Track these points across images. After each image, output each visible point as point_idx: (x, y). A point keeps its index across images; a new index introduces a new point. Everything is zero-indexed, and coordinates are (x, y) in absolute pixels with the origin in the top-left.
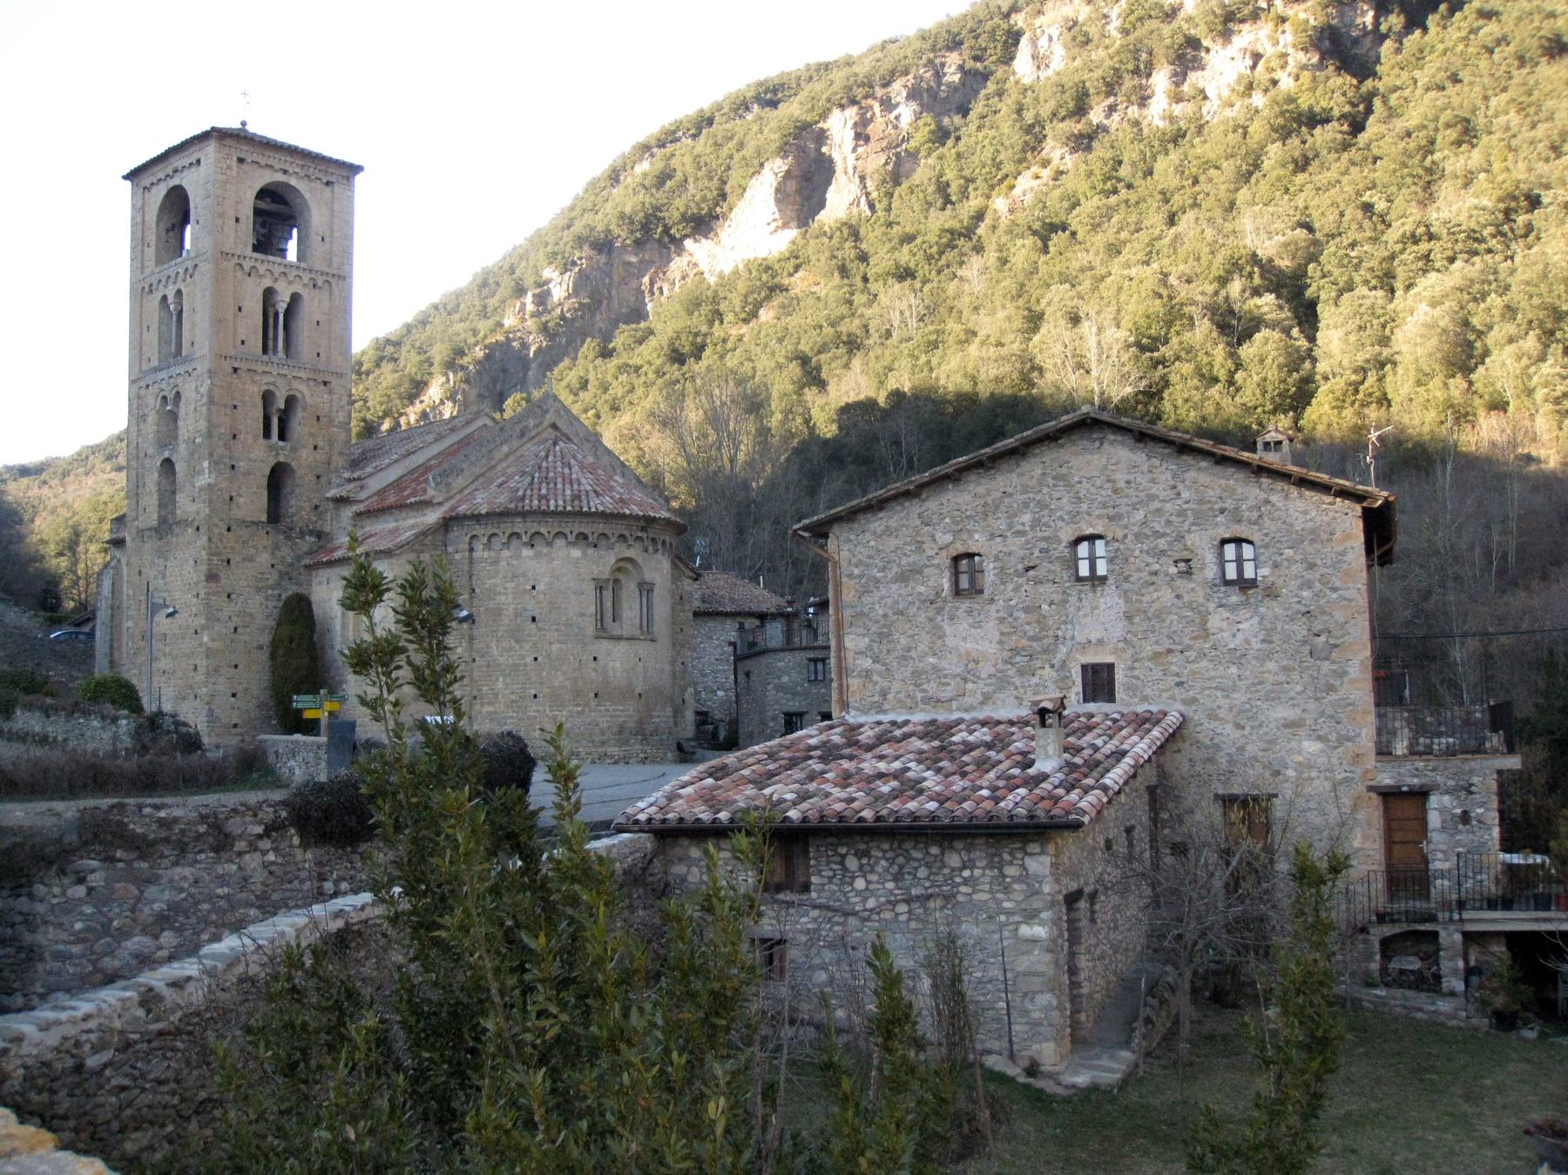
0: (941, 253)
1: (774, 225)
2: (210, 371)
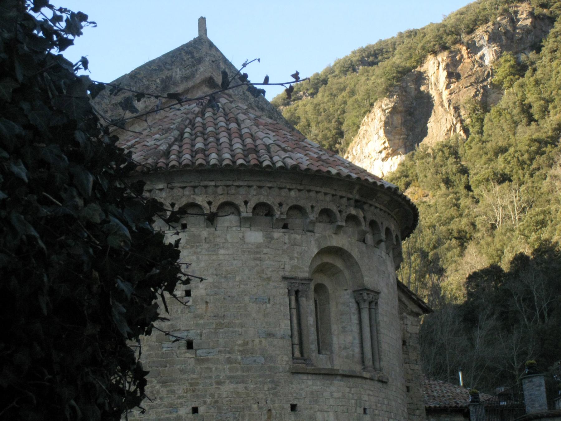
0: (532, 159)
1: (384, 154)
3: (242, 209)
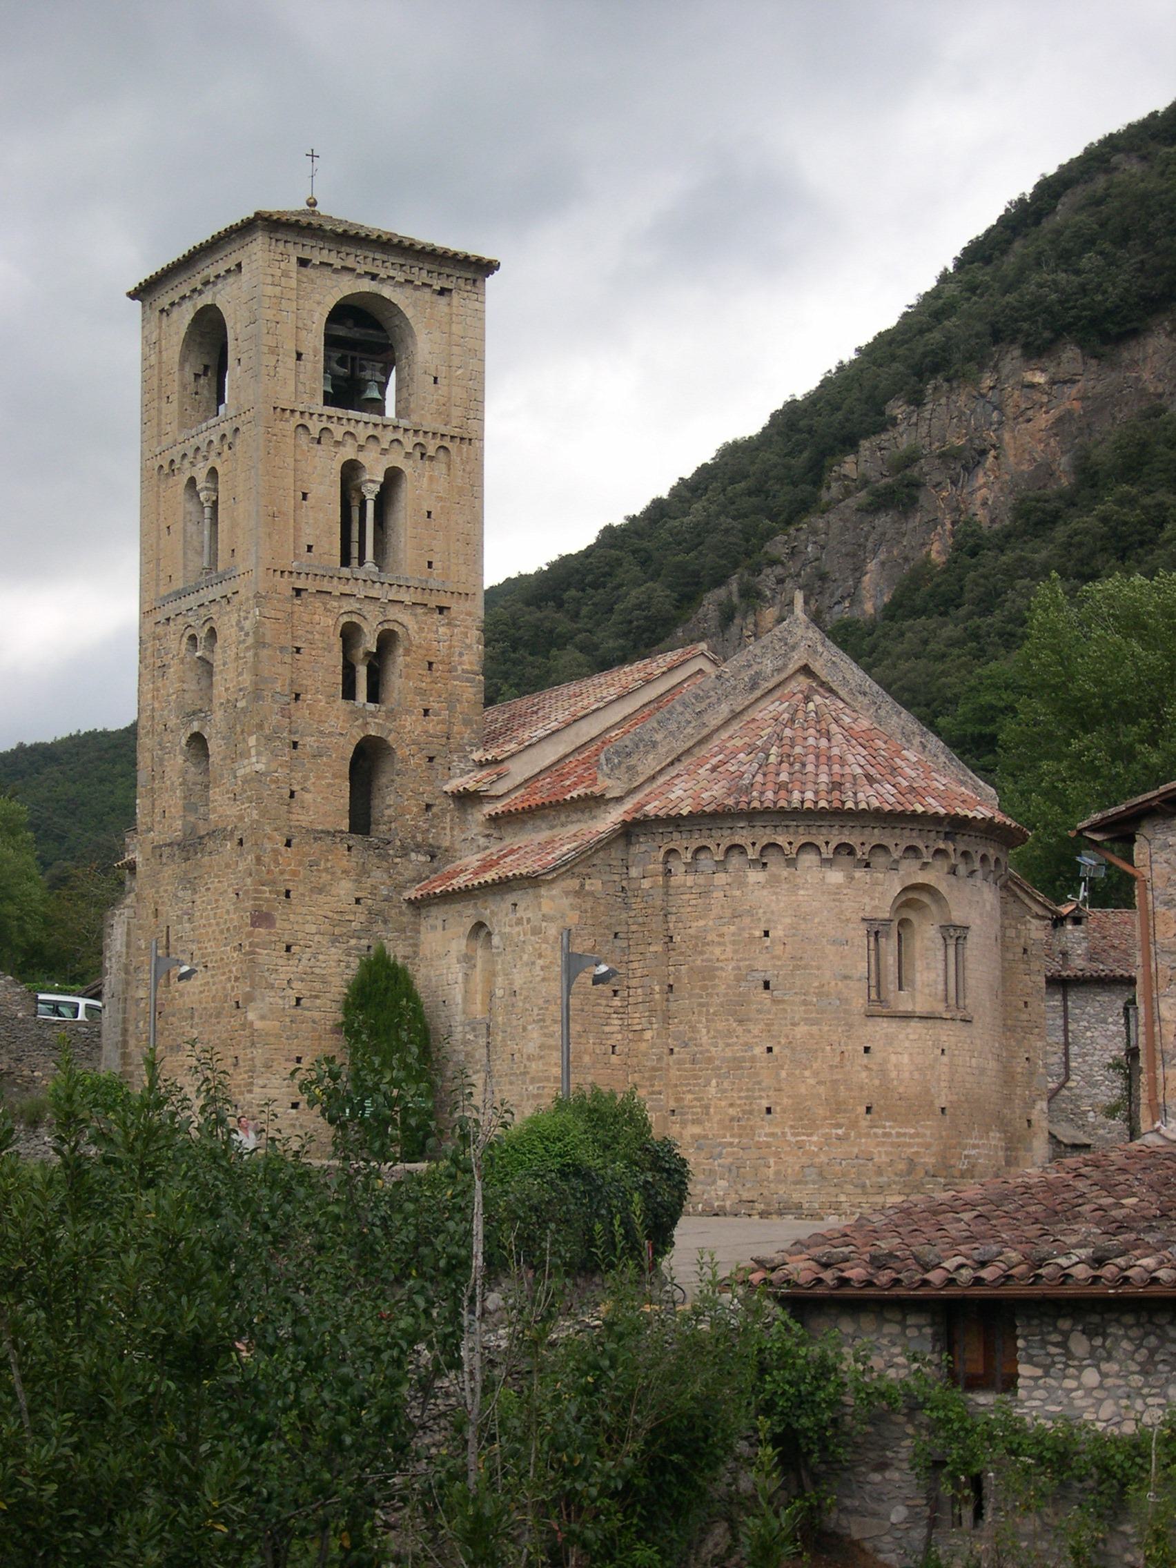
2: (257, 596)
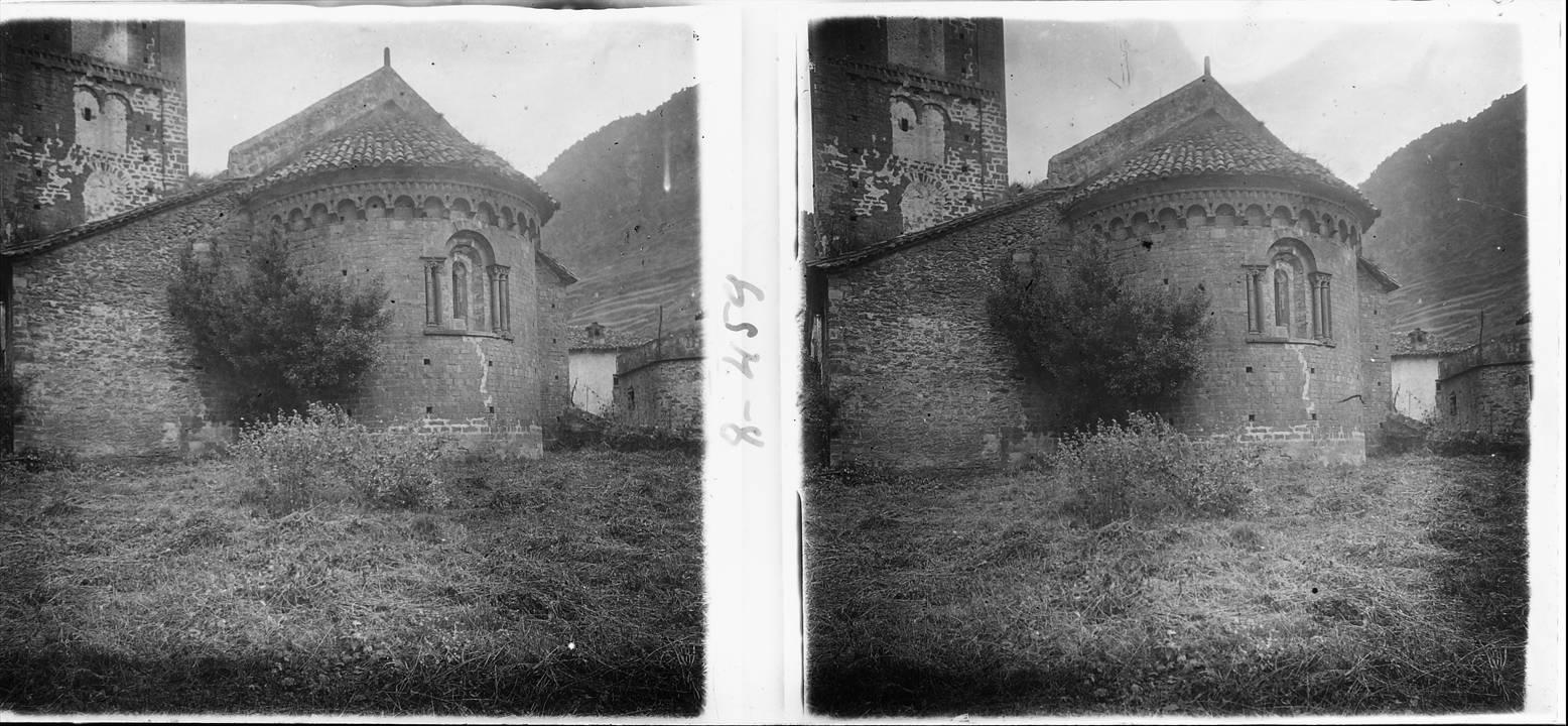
3: (1208, 210)
